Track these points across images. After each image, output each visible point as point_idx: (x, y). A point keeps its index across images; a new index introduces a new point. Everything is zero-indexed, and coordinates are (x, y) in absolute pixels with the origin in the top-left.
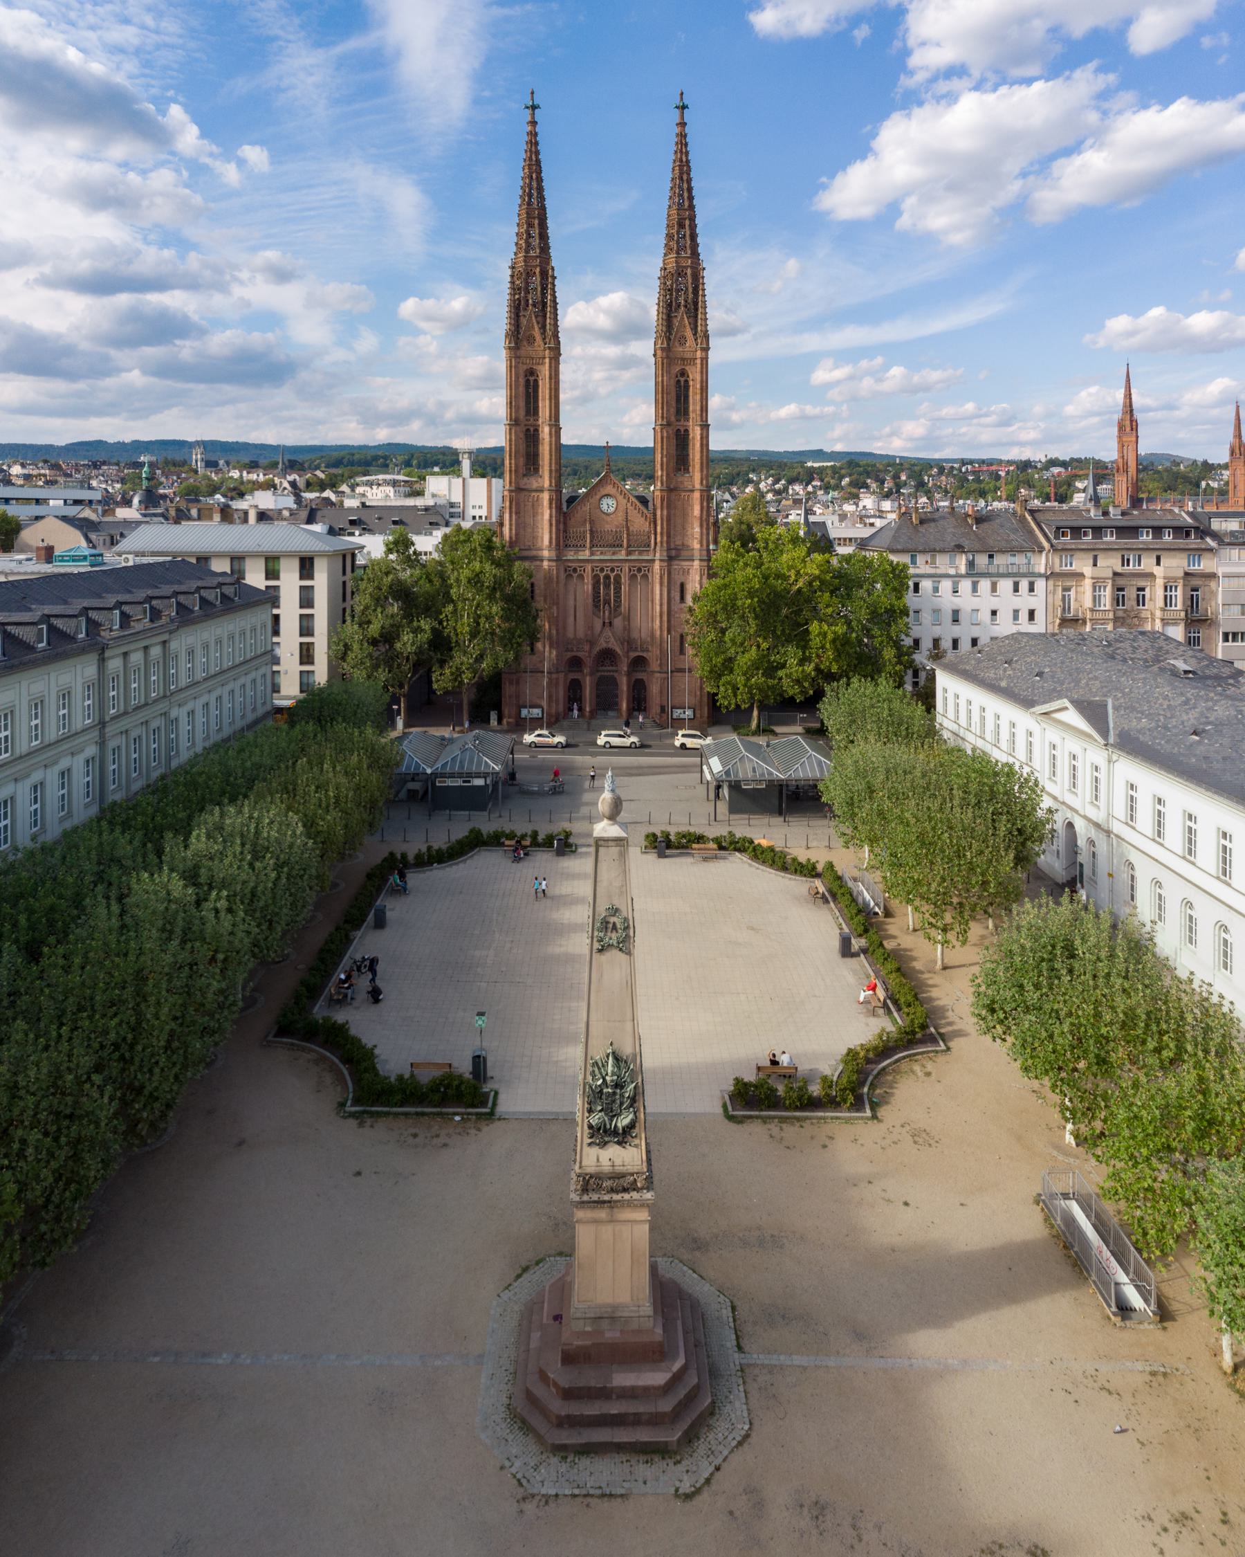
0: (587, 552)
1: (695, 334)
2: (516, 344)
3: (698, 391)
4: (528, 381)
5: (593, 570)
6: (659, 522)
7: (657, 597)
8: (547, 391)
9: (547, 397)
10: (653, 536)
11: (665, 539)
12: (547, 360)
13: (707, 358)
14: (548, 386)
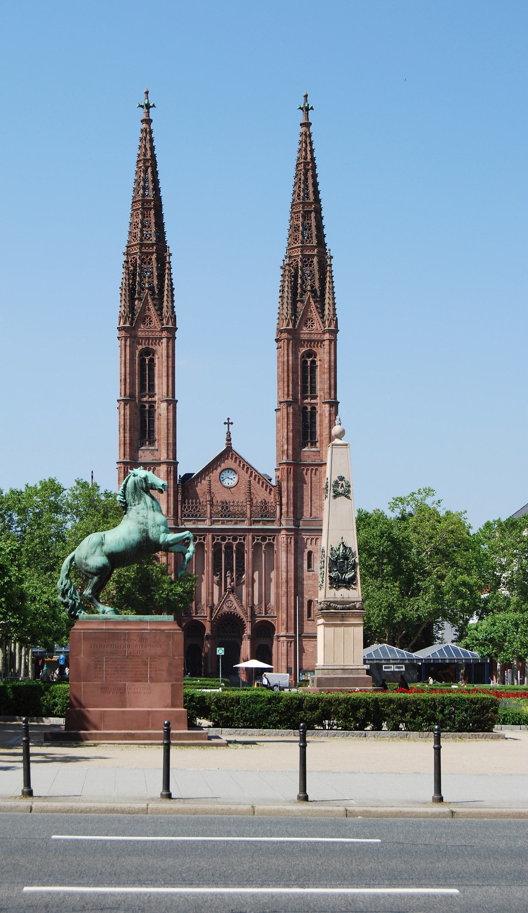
0: (208, 522)
1: (322, 317)
2: (131, 324)
3: (327, 371)
4: (142, 361)
5: (213, 539)
6: (284, 494)
7: (284, 564)
8: (165, 369)
9: (165, 374)
10: (278, 507)
11: (291, 509)
12: (164, 340)
13: (335, 340)
14: (165, 364)
